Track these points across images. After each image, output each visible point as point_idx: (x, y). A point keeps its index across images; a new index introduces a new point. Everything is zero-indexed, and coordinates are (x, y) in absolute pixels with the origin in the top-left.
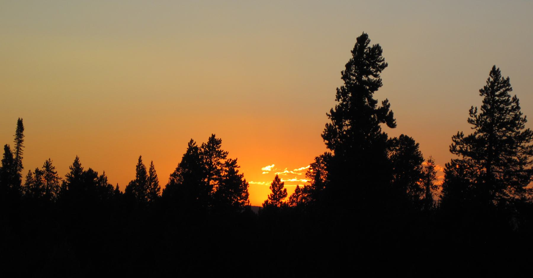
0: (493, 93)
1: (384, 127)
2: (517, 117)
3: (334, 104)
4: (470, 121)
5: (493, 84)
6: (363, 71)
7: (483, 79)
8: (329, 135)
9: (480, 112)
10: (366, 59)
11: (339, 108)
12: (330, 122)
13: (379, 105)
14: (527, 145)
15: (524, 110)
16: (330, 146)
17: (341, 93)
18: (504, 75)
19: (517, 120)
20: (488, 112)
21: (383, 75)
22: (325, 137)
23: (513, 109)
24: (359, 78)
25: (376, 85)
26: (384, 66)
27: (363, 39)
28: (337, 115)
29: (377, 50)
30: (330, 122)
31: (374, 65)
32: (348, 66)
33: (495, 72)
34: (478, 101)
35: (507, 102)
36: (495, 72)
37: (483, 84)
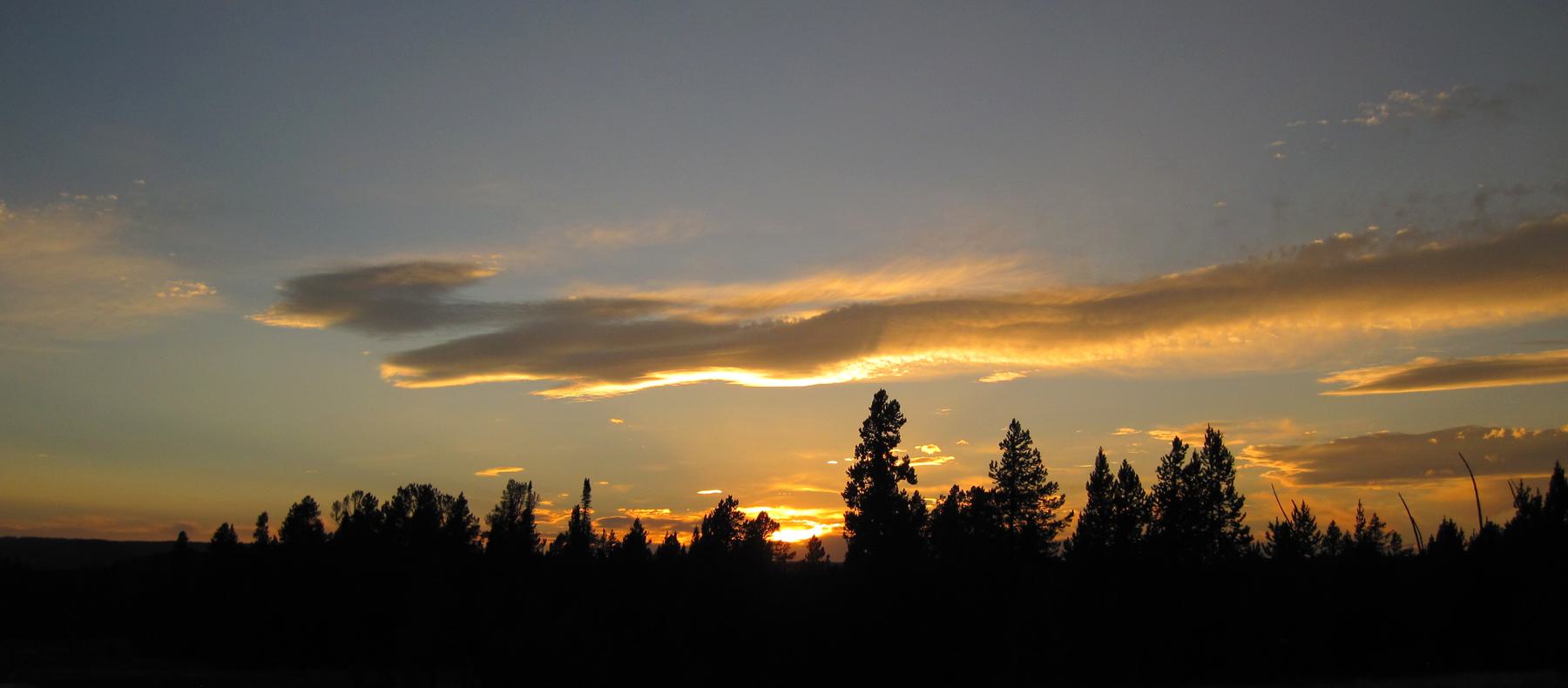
0: (1014, 445)
1: (902, 485)
2: (1038, 471)
3: (852, 461)
4: (991, 475)
5: (1012, 439)
6: (881, 429)
7: (1004, 432)
8: (850, 494)
9: (1000, 466)
10: (884, 416)
11: (858, 467)
12: (851, 480)
13: (899, 463)
14: (1048, 498)
15: (1047, 463)
16: (851, 505)
17: (860, 451)
18: (1024, 428)
19: (1038, 475)
20: (1008, 466)
21: (902, 430)
22: (845, 496)
23: (1035, 462)
24: (878, 436)
25: (894, 442)
26: (903, 421)
27: (881, 396)
28: (856, 473)
29: (895, 406)
30: (851, 480)
31: (892, 420)
32: (866, 423)
33: (1015, 426)
34: (998, 454)
35: (1028, 456)
36: (1015, 426)
37: (1003, 437)
